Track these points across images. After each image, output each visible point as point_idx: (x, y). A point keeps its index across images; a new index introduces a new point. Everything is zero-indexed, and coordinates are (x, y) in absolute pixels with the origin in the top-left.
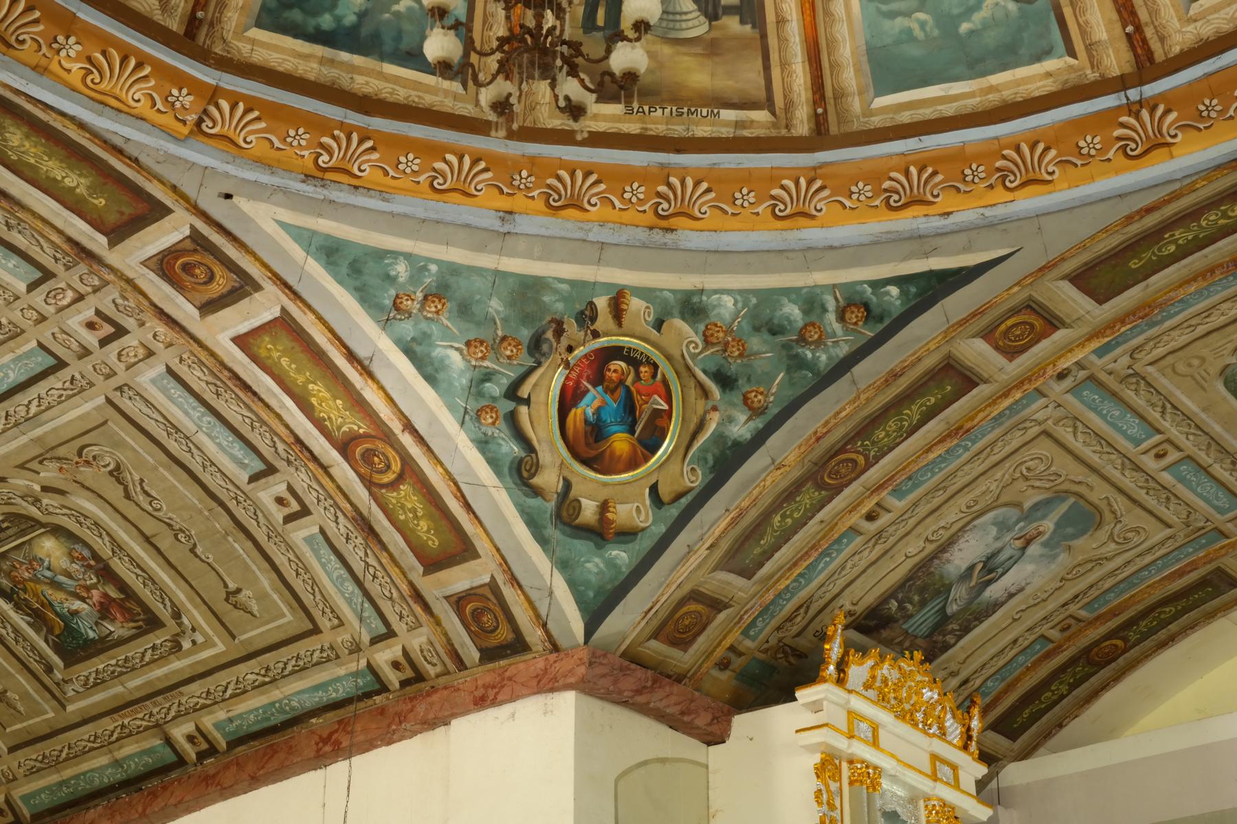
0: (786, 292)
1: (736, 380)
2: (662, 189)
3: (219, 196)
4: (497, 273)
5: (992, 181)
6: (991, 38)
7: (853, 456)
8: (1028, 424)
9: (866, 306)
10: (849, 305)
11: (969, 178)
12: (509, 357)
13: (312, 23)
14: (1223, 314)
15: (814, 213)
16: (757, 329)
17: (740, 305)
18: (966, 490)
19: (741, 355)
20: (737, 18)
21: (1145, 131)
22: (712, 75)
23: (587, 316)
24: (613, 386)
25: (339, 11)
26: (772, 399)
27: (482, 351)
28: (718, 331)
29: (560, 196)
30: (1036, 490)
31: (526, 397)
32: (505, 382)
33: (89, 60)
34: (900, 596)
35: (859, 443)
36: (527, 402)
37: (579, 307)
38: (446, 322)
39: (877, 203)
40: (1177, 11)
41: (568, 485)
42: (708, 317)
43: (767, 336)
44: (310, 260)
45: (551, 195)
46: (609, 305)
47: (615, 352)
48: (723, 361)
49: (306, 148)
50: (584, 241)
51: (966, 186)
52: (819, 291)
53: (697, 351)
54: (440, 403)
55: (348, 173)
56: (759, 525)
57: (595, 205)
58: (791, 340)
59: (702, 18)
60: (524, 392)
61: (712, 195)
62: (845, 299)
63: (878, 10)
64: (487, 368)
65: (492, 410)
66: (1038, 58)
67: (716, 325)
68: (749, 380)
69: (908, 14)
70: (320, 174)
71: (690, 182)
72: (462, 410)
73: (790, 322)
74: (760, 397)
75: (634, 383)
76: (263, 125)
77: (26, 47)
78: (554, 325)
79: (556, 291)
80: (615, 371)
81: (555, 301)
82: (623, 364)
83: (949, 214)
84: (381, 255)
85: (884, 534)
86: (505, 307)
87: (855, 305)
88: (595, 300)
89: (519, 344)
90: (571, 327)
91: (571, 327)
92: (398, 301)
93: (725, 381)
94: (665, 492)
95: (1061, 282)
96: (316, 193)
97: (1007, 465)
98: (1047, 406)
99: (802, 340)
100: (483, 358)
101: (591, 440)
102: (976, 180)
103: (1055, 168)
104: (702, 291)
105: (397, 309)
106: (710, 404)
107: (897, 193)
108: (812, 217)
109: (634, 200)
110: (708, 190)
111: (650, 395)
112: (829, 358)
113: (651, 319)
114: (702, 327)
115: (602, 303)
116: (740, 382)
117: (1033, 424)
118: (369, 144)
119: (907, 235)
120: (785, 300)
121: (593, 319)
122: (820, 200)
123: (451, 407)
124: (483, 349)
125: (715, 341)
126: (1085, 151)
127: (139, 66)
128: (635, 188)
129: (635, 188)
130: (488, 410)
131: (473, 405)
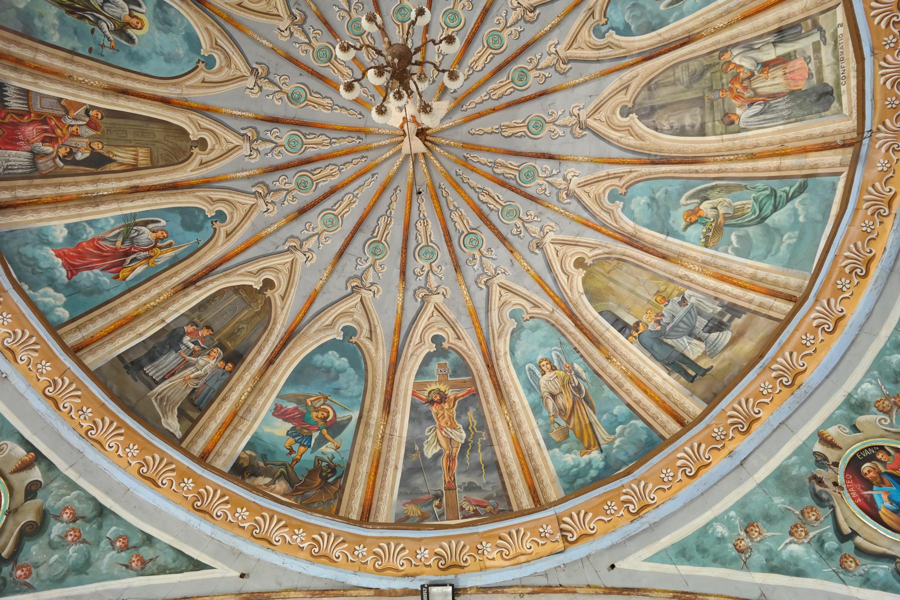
0: (882, 353)
2: (774, 374)
3: (609, 571)
4: (761, 485)
5: (878, 221)
6: (813, 209)
11: (869, 230)
12: (817, 520)
13: (588, 478)
15: (841, 314)
17: (873, 381)
20: (736, 319)
21: (886, 138)
22: (751, 340)
23: (821, 461)
24: (878, 480)
25: (594, 466)
27: (802, 531)
28: (883, 403)
29: (741, 423)
31: (850, 531)
32: (831, 534)
33: (497, 546)
36: (854, 534)
37: (812, 460)
38: (769, 534)
39: (856, 281)
40: (843, 121)
42: (869, 402)
44: (680, 567)
46: (822, 444)
47: (855, 464)
49: (620, 509)
50: (775, 430)
51: (873, 234)
52: (894, 338)
53: (889, 421)
54: (820, 581)
55: (648, 505)
57: (759, 412)
59: (725, 332)
60: (846, 530)
61: (795, 354)
63: (772, 256)
64: (814, 536)
65: (846, 557)
66: (834, 189)
67: (878, 401)
69: (782, 242)
70: (638, 516)
71: (780, 360)
72: (833, 573)
75: (885, 467)
76: (590, 515)
77: (469, 562)
78: (814, 481)
79: (793, 465)
80: (869, 471)
81: (800, 468)
83: (885, 248)
84: (704, 531)
86: (783, 497)
88: (815, 450)
89: (812, 508)
90: (821, 473)
91: (821, 473)
92: (738, 547)
96: (642, 524)
100: (807, 534)
102: (873, 227)
104: (850, 395)
105: (742, 552)
108: (844, 316)
109: (770, 391)
110: (791, 354)
113: (848, 430)
114: (874, 409)
115: (818, 447)
118: (643, 483)
119: (885, 276)
120: (887, 358)
121: (826, 459)
122: (835, 306)
123: (828, 578)
124: (801, 529)
125: (889, 408)
126: (885, 169)
127: (518, 532)
128: (763, 386)
129: (763, 386)
130: (845, 560)
131: (835, 565)
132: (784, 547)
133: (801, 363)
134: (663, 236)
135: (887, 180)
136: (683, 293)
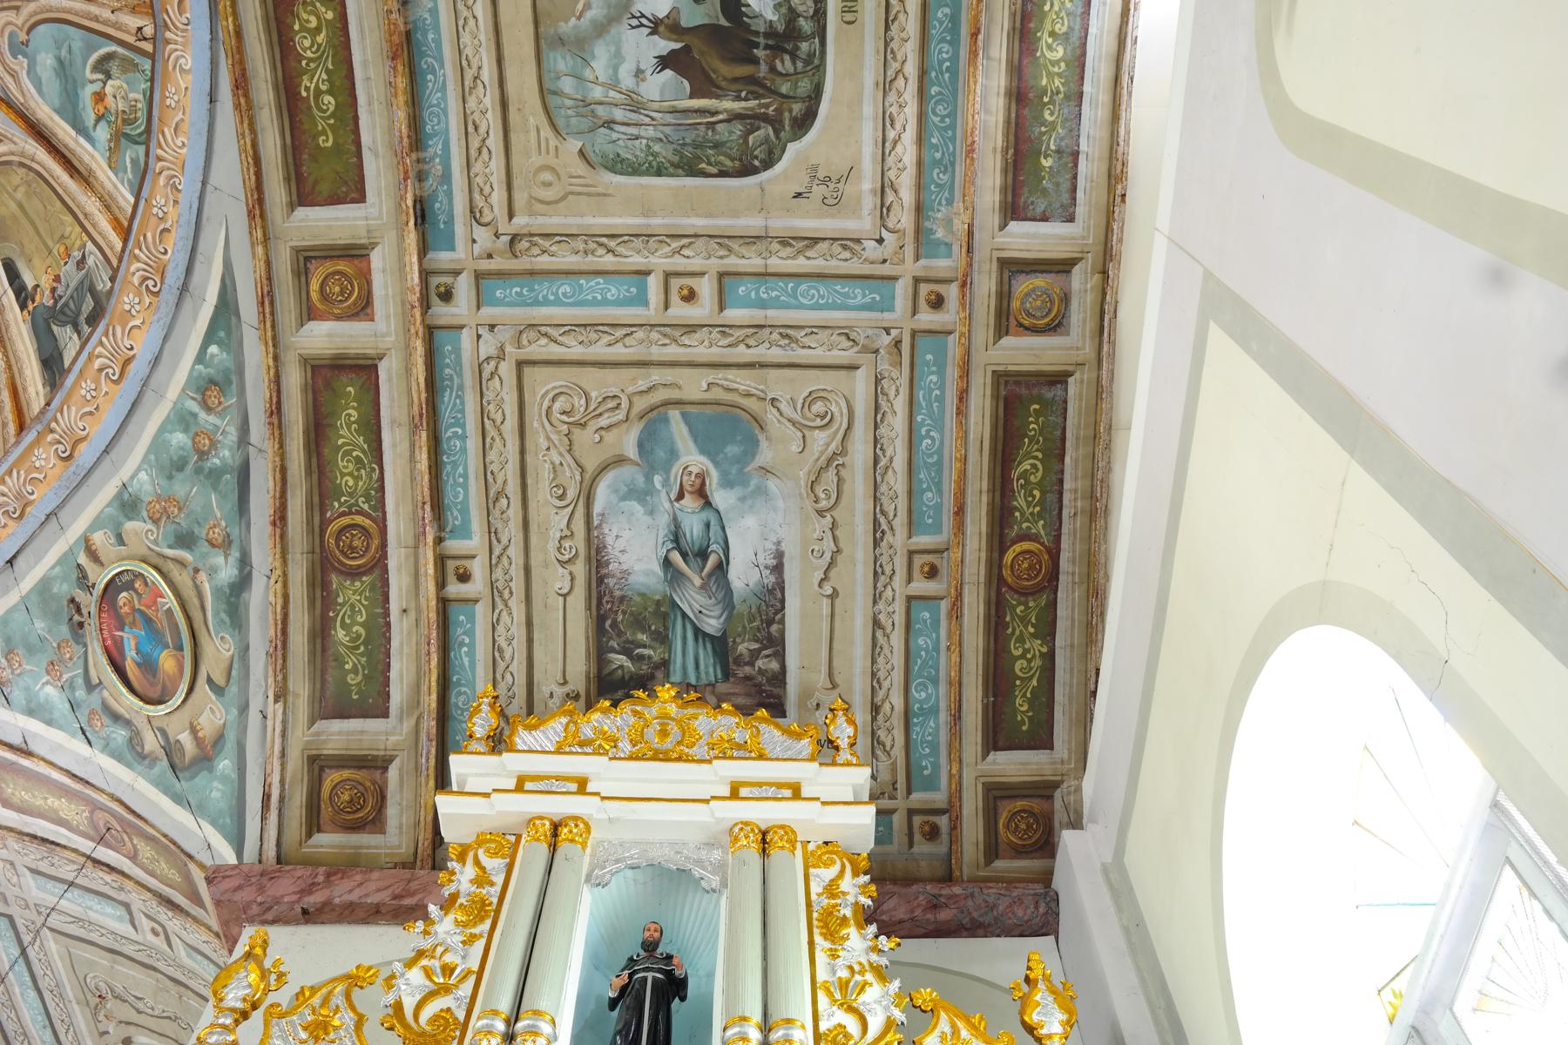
0: (162, 429)
1: (193, 533)
5: (171, 198)
7: (346, 521)
8: (488, 369)
9: (212, 382)
10: (204, 395)
12: (71, 659)
14: (484, 113)
15: (131, 353)
16: (170, 477)
18: (529, 481)
19: (180, 509)
26: (223, 524)
30: (615, 431)
32: (80, 681)
34: (614, 644)
35: (336, 504)
37: (74, 576)
38: (28, 667)
39: (147, 301)
41: (163, 732)
43: (180, 476)
45: (8, 511)
48: (174, 526)
52: (179, 406)
56: (324, 650)
58: (196, 462)
62: (196, 392)
67: (151, 503)
68: (198, 523)
73: (182, 448)
74: (217, 530)
82: (124, 594)
85: (500, 585)
87: (206, 389)
93: (185, 540)
94: (219, 679)
95: (295, 213)
97: (536, 424)
98: (479, 337)
99: (203, 455)
101: (151, 679)
103: (180, 139)
106: (190, 569)
107: (148, 278)
111: (155, 603)
112: (231, 449)
113: (113, 540)
114: (145, 514)
115: (83, 559)
116: (196, 531)
117: (493, 363)
122: (123, 342)
132: (41, 688)
133: (80, 425)
134: (73, 133)
135: (177, 125)
136: (84, 246)
